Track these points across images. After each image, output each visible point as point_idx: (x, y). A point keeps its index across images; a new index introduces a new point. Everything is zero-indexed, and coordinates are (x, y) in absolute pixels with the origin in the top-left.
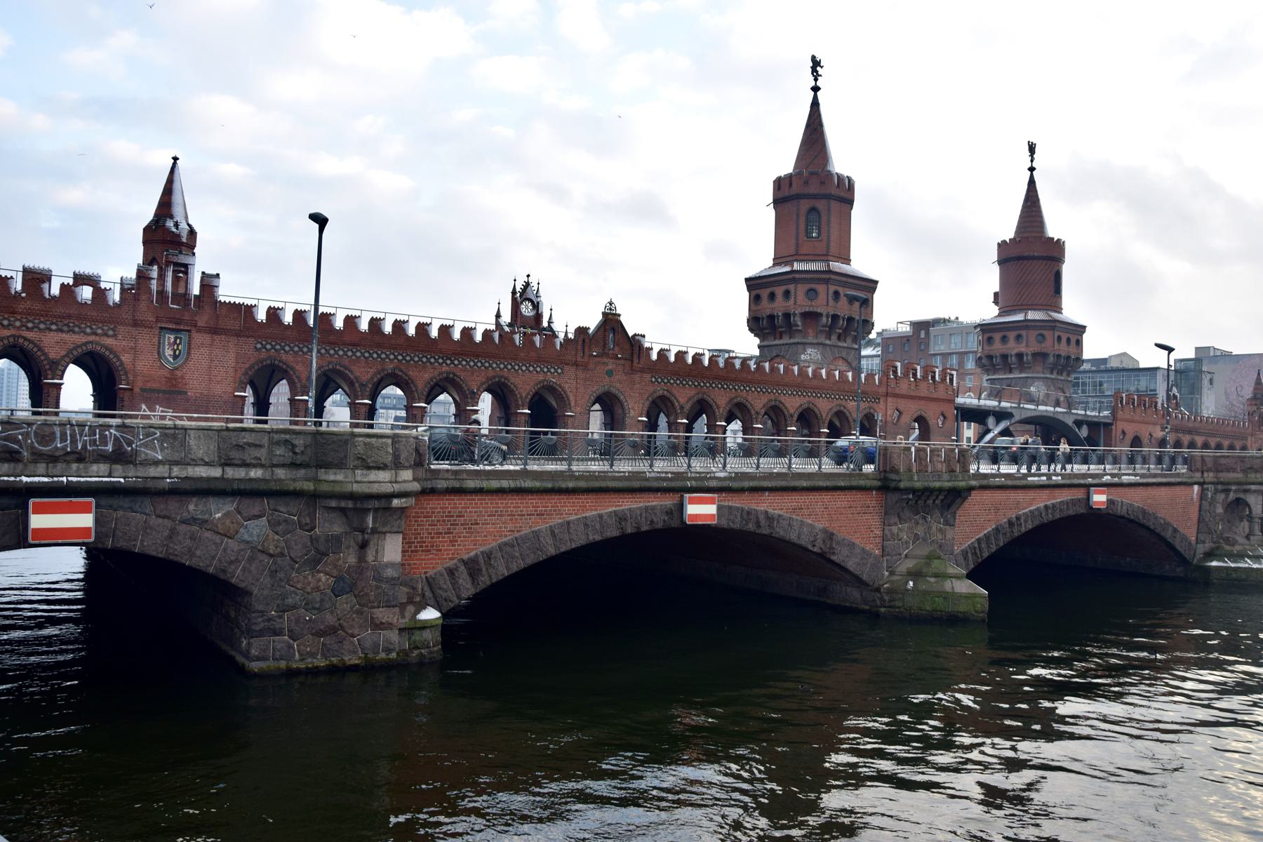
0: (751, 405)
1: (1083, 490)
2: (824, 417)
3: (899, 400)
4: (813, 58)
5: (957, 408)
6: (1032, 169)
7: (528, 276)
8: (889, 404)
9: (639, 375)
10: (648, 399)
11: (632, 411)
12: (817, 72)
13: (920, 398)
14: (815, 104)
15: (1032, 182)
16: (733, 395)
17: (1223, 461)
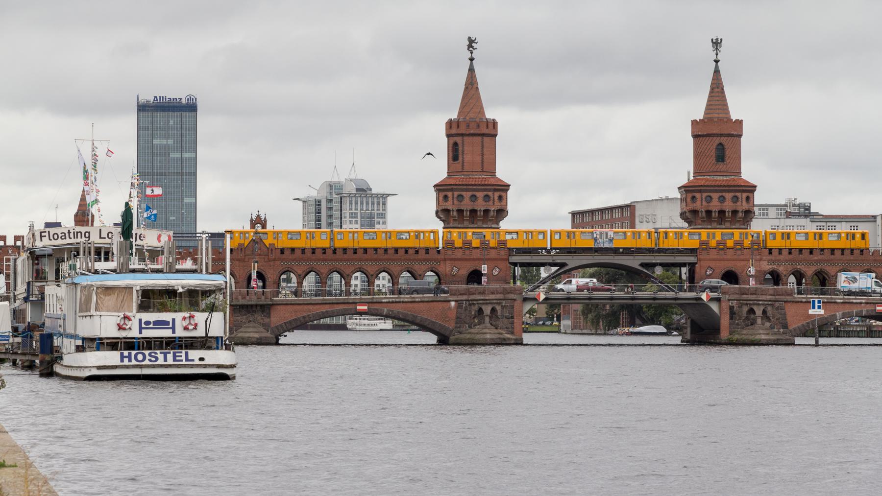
0: (343, 271)
1: (354, 305)
2: (396, 275)
3: (456, 262)
4: (469, 38)
5: (511, 263)
6: (717, 61)
7: (258, 211)
8: (447, 264)
9: (273, 262)
10: (279, 273)
11: (270, 280)
13: (474, 259)
14: (471, 70)
15: (717, 72)
17: (471, 290)
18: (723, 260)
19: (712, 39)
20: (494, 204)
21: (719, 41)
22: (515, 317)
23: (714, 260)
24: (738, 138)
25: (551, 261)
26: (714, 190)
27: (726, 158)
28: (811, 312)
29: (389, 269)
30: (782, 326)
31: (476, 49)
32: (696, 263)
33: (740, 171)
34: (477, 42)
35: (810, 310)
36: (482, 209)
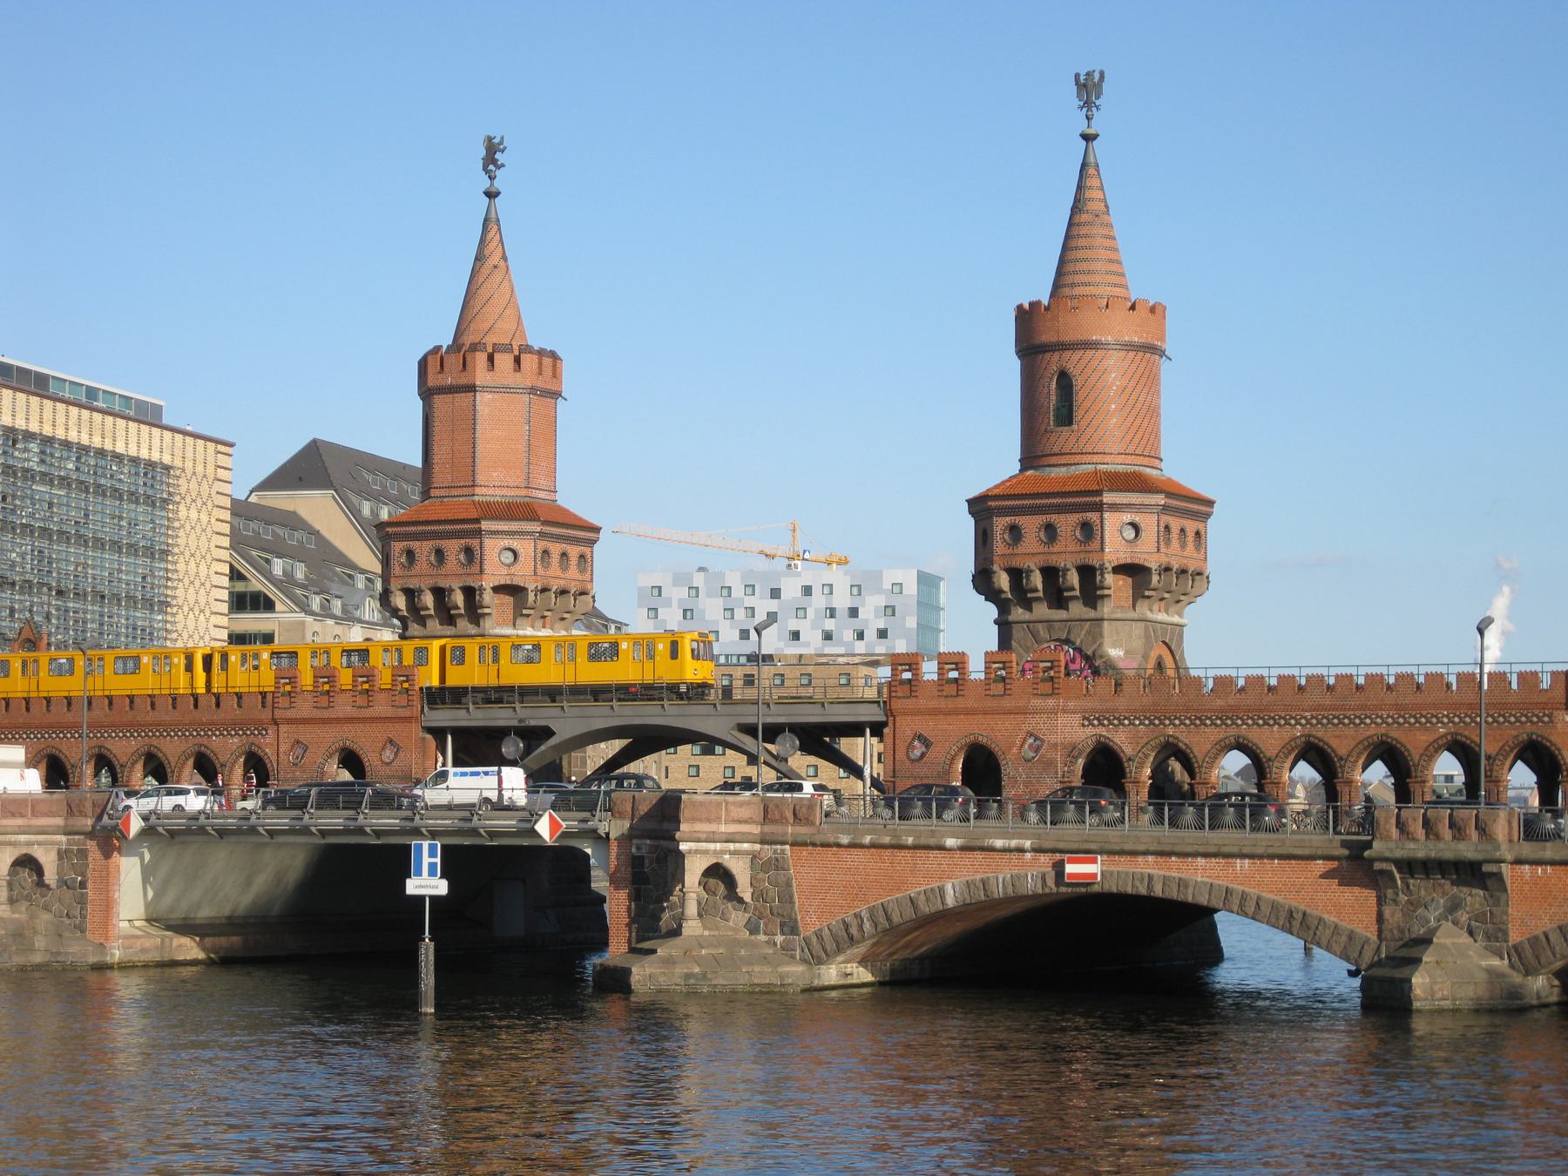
2: (173, 764)
4: (490, 139)
5: (430, 730)
12: (494, 162)
13: (338, 721)
16: (43, 746)
18: (956, 712)
19: (1077, 76)
20: (481, 572)
21: (1097, 77)
22: (89, 885)
23: (934, 712)
24: (1148, 355)
25: (515, 723)
26: (1031, 507)
27: (1078, 415)
28: (413, 887)
29: (159, 750)
30: (782, 925)
31: (503, 165)
32: (885, 724)
33: (1158, 448)
34: (505, 148)
35: (408, 881)
36: (456, 584)
